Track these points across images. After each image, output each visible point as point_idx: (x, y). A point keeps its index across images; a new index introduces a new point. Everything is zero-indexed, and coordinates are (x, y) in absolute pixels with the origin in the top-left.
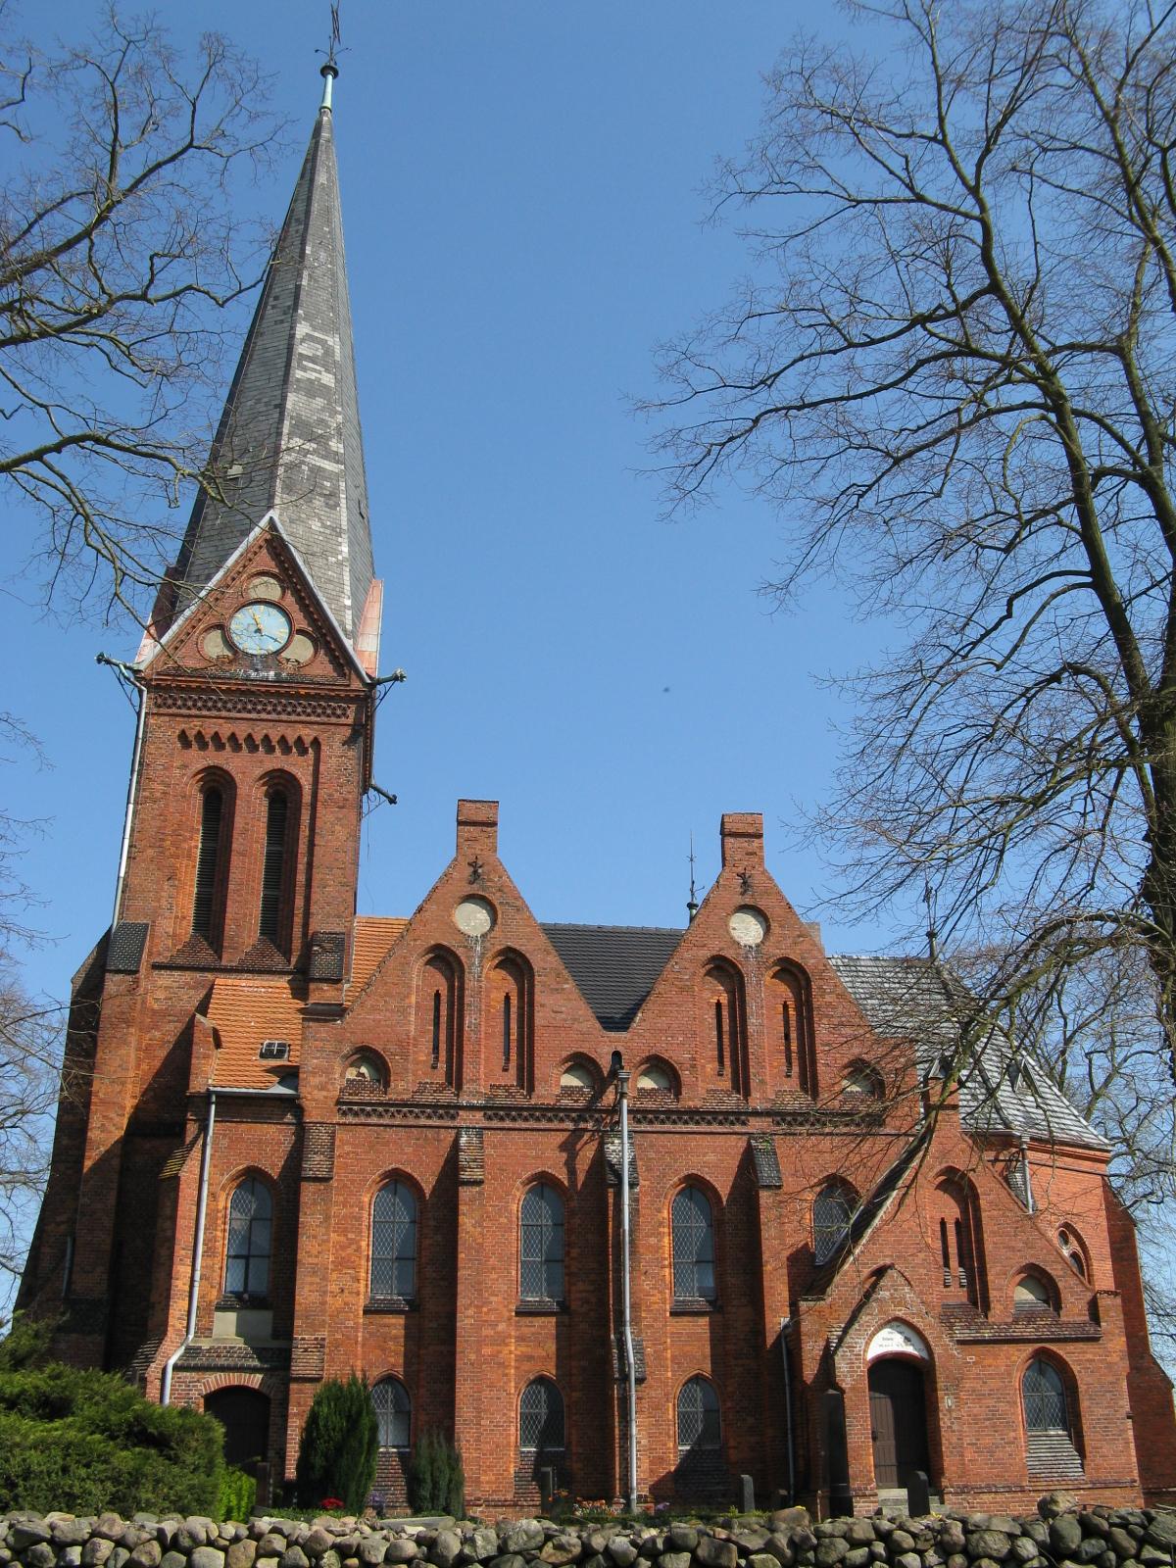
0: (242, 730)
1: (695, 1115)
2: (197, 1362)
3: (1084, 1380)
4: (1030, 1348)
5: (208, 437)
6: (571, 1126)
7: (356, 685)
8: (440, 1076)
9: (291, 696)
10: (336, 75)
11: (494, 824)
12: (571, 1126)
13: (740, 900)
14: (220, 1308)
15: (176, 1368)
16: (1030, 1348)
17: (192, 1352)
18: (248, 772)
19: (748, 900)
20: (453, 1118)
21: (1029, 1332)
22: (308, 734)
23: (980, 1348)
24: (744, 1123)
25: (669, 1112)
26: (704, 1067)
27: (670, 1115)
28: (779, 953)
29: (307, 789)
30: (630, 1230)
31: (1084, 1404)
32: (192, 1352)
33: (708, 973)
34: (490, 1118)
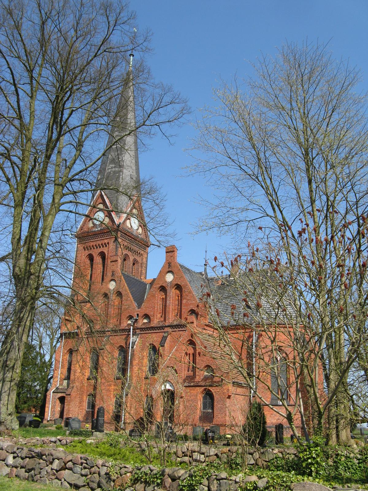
0: (94, 244)
1: (153, 328)
2: (58, 391)
3: (216, 397)
4: (203, 388)
5: (139, 156)
6: (127, 333)
7: (115, 227)
8: (162, 319)
9: (104, 233)
10: (133, 56)
11: (167, 252)
12: (127, 333)
13: (168, 270)
14: (65, 379)
15: (53, 392)
16: (203, 388)
17: (57, 388)
18: (95, 253)
19: (170, 270)
20: (164, 329)
21: (203, 384)
22: (106, 241)
23: (191, 388)
24: (164, 329)
25: (147, 328)
26: (157, 315)
27: (148, 329)
28: (176, 283)
29: (107, 255)
30: (131, 359)
31: (215, 403)
32: (57, 388)
33: (160, 291)
34: (141, 331)
